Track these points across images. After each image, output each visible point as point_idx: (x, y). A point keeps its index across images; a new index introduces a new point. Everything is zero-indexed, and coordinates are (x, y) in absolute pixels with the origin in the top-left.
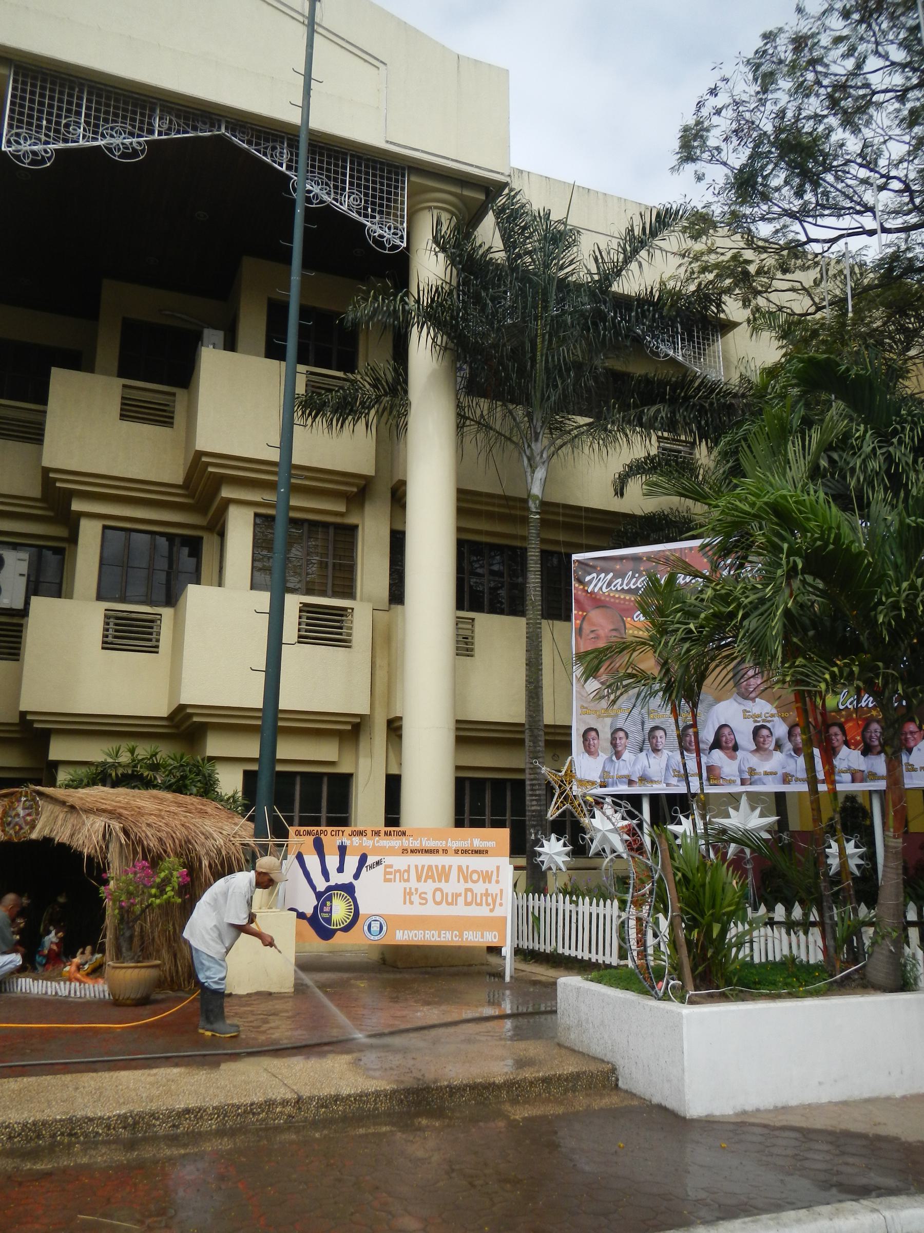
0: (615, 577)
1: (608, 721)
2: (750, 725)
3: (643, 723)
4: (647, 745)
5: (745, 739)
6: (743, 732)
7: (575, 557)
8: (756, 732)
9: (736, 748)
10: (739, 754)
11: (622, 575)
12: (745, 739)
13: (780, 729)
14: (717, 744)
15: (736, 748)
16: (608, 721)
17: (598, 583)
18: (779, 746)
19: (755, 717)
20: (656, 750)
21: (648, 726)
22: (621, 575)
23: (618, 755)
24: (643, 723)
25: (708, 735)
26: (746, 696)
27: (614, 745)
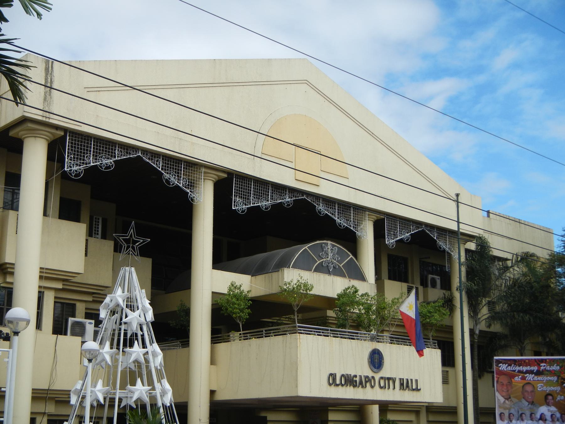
0: (508, 366)
1: (507, 411)
2: (550, 414)
3: (518, 412)
4: (520, 419)
5: (548, 417)
6: (548, 415)
7: (495, 358)
8: (552, 416)
9: (546, 420)
10: (547, 422)
11: (511, 365)
12: (548, 417)
13: (558, 415)
14: (541, 419)
15: (546, 420)
16: (507, 411)
17: (503, 367)
18: (558, 420)
19: (551, 411)
20: (523, 420)
21: (520, 412)
22: (510, 365)
23: (511, 421)
24: (518, 412)
25: (538, 416)
26: (548, 405)
27: (510, 418)
